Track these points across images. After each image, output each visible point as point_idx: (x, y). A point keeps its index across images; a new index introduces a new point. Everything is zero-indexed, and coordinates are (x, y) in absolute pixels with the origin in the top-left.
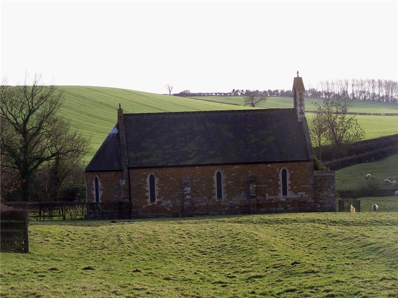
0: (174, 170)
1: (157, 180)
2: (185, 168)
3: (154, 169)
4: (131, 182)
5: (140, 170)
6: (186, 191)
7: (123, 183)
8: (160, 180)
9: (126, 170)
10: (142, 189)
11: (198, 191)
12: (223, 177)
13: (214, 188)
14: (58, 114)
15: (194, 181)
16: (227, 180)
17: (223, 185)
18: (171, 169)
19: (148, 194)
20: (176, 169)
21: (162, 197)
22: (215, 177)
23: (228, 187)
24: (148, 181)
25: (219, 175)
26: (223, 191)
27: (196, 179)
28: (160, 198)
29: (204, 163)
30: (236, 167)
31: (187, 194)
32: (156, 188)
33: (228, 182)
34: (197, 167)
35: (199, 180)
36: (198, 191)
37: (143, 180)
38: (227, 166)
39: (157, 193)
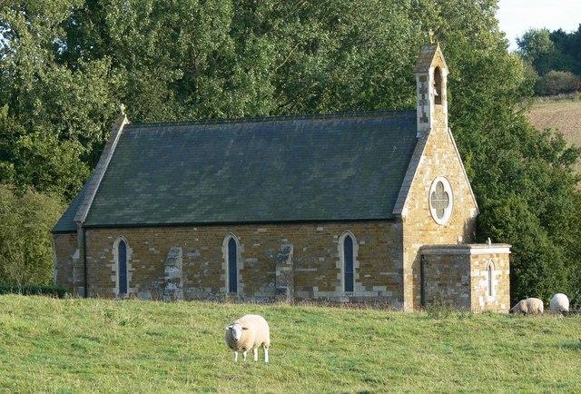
0: (157, 233)
1: (129, 251)
2: (176, 229)
3: (125, 231)
4: (88, 253)
5: (103, 231)
6: (167, 275)
7: (77, 255)
8: (135, 251)
9: (80, 232)
10: (106, 268)
11: (196, 276)
12: (240, 249)
13: (339, 270)
14: (551, 32)
15: (190, 255)
16: (245, 256)
17: (240, 266)
18: (152, 230)
19: (116, 279)
20: (160, 230)
21: (137, 285)
22: (225, 250)
23: (247, 267)
24: (116, 252)
25: (232, 243)
26: (239, 277)
27: (193, 252)
28: (134, 286)
29: (205, 221)
30: (262, 230)
31: (169, 281)
32: (129, 267)
33: (248, 260)
34: (195, 229)
35: (198, 254)
36: (196, 276)
37: (107, 250)
38: (246, 227)
39: (129, 279)
